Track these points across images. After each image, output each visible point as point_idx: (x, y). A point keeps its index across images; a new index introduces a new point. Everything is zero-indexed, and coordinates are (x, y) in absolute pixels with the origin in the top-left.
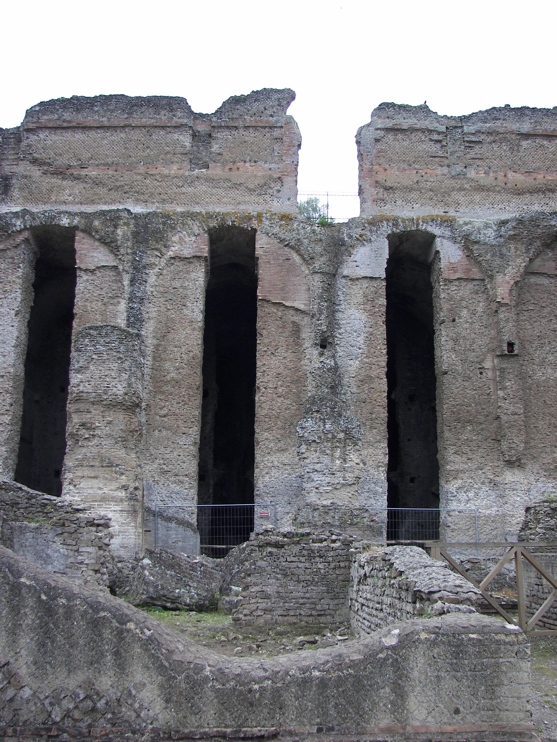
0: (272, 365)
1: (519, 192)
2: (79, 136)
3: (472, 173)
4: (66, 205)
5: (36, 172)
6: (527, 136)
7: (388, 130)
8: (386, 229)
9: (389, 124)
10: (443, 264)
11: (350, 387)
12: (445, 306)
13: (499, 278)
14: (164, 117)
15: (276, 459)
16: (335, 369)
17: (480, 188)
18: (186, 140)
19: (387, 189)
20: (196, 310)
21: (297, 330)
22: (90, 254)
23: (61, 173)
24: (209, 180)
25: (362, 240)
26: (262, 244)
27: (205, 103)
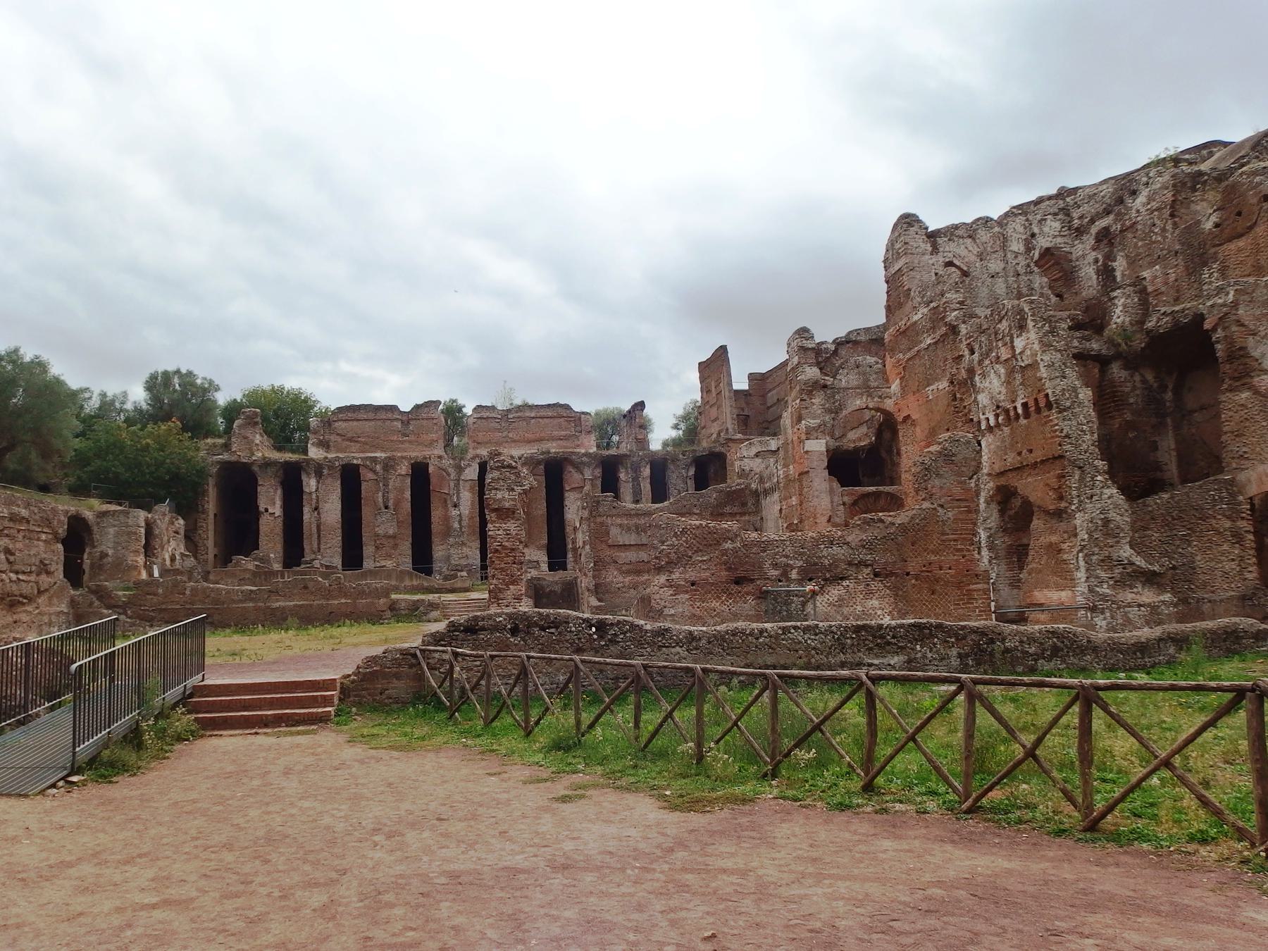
0: (436, 514)
1: (529, 442)
2: (355, 423)
4: (355, 456)
5: (339, 439)
8: (478, 460)
14: (390, 415)
15: (440, 548)
17: (514, 441)
18: (399, 424)
20: (408, 494)
21: (445, 501)
22: (366, 475)
23: (351, 440)
24: (410, 442)
25: (469, 465)
26: (431, 469)
27: (406, 407)
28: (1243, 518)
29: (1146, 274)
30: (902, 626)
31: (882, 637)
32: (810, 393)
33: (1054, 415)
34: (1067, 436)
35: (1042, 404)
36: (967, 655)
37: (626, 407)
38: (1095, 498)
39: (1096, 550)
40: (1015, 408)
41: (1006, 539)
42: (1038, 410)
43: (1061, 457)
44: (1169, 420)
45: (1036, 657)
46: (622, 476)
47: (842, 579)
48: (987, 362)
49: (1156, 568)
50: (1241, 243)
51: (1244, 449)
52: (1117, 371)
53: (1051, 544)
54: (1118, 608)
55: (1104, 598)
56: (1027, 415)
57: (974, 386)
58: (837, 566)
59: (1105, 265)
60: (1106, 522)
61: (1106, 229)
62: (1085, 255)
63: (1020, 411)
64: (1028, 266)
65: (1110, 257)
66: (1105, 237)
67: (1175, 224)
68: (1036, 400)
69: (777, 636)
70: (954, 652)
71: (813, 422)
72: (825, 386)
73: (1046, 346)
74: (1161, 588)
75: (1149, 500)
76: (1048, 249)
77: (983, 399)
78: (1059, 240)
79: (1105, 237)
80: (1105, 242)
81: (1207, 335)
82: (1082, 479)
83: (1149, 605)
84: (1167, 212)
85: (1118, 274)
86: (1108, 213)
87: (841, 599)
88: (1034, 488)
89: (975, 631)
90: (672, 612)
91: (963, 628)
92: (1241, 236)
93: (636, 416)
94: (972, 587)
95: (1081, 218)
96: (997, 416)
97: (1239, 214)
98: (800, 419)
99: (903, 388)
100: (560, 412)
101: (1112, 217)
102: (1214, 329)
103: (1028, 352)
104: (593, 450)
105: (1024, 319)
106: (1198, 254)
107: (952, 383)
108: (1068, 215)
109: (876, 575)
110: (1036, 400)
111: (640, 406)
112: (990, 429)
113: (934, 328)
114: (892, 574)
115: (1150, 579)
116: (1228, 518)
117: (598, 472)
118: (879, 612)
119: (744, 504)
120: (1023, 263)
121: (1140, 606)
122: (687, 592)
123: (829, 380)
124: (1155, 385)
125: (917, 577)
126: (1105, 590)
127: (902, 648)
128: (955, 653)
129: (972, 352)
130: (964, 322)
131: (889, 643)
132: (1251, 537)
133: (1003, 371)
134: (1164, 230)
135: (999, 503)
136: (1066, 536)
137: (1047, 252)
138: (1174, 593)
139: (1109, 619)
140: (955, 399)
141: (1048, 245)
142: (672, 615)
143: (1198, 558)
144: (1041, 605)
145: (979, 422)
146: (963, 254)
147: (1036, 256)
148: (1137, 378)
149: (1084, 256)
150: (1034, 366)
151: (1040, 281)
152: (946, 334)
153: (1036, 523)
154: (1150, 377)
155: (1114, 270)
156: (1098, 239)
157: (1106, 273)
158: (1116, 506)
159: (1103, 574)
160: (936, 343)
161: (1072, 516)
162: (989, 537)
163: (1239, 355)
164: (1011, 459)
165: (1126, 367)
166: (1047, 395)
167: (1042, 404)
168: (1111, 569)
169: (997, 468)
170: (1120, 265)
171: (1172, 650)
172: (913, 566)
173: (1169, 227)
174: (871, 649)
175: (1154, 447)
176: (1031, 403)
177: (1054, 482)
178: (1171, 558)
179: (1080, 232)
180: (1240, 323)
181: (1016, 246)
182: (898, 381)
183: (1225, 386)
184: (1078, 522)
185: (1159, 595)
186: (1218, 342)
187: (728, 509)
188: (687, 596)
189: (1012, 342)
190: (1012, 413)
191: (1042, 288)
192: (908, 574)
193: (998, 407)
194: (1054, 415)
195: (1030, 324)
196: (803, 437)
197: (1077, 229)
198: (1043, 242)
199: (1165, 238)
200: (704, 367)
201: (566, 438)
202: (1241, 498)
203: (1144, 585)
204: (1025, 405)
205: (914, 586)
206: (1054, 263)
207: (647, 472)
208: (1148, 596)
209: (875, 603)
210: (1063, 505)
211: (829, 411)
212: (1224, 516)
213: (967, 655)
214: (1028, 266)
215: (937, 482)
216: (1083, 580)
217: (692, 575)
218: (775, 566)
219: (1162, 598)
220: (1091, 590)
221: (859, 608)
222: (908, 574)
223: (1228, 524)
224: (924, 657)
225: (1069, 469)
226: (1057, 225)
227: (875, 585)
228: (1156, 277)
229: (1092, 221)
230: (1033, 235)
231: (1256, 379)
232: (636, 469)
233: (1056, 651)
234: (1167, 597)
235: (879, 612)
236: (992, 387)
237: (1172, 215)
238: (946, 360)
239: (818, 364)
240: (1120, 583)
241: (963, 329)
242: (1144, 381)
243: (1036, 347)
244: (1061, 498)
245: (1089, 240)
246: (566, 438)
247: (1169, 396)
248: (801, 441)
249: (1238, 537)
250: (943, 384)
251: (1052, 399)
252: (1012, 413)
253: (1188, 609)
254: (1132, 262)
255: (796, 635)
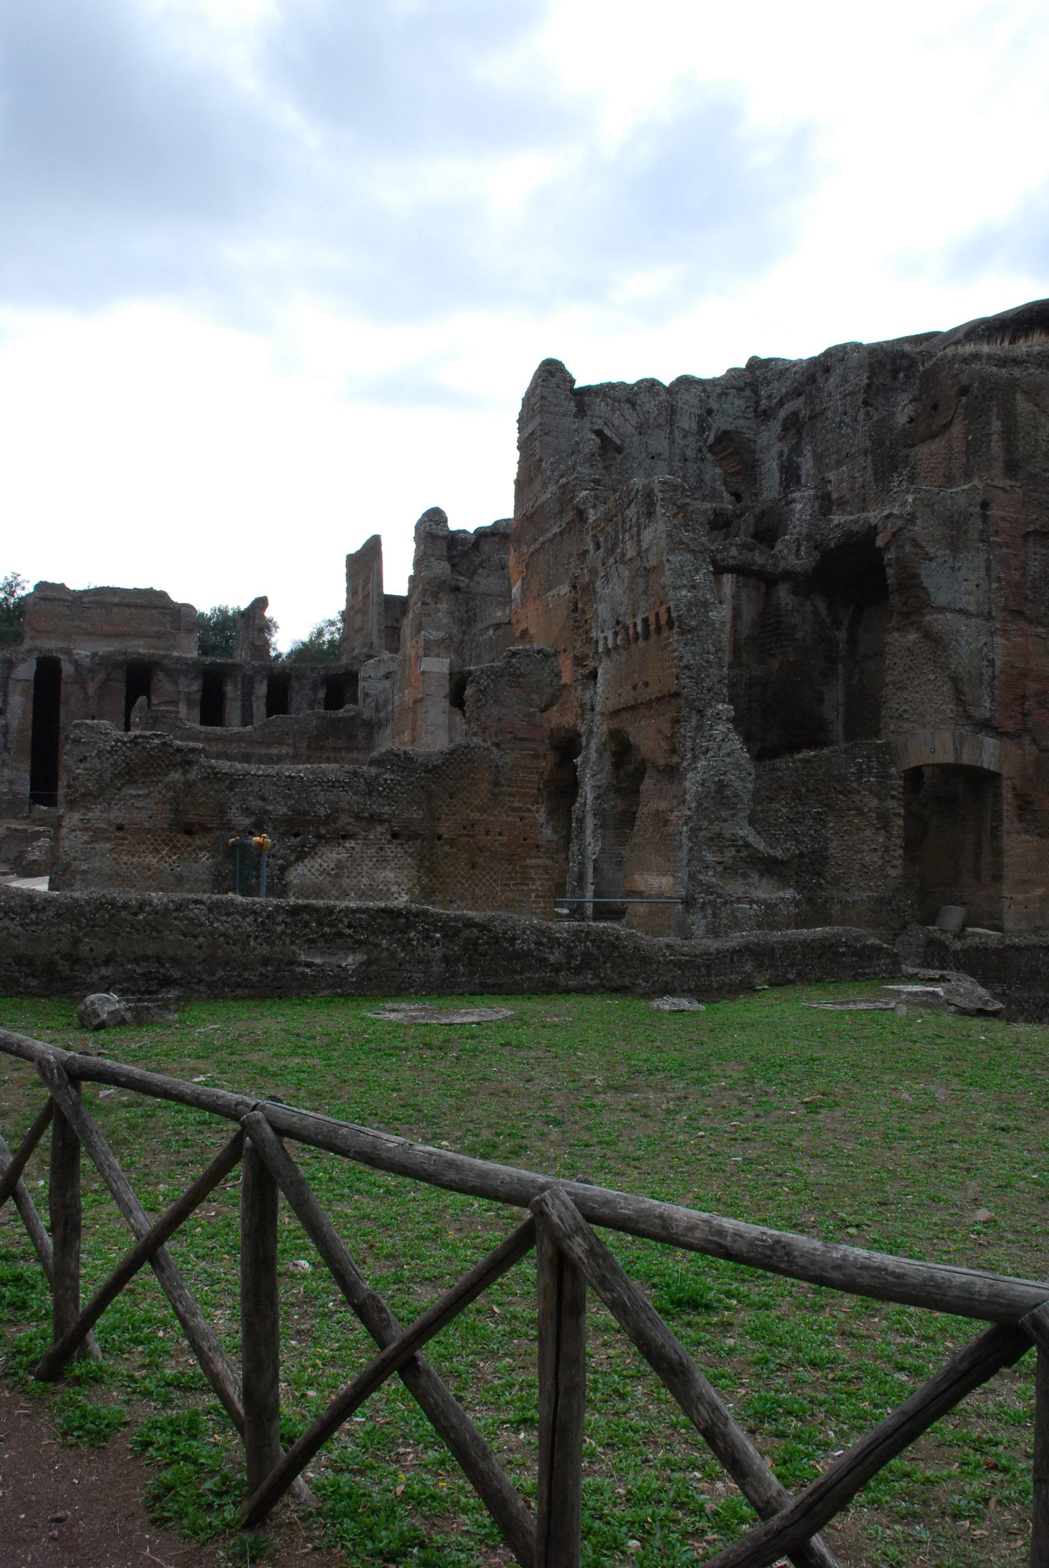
1: (108, 636)
3: (84, 625)
6: (116, 605)
7: (41, 599)
8: (36, 655)
9: (42, 595)
10: (64, 674)
11: (13, 735)
12: (63, 695)
13: (90, 683)
16: (6, 725)
17: (88, 633)
19: (39, 632)
25: (23, 660)
28: (893, 797)
29: (831, 476)
30: (367, 911)
31: (331, 925)
32: (435, 596)
33: (674, 636)
34: (687, 667)
35: (663, 621)
36: (457, 959)
37: (244, 605)
38: (711, 754)
39: (705, 824)
40: (635, 625)
41: (619, 802)
42: (659, 629)
43: (677, 695)
44: (840, 666)
45: (556, 969)
46: (229, 689)
47: (345, 837)
48: (611, 560)
49: (779, 853)
50: (934, 445)
51: (905, 707)
52: (784, 594)
53: (657, 812)
54: (724, 904)
55: (708, 889)
56: (647, 636)
57: (595, 592)
58: (337, 818)
59: (790, 460)
60: (721, 786)
61: (795, 414)
62: (770, 446)
63: (639, 629)
64: (700, 450)
65: (796, 450)
66: (793, 425)
67: (868, 414)
68: (657, 614)
69: (166, 912)
70: (439, 952)
71: (436, 635)
72: (457, 589)
73: (677, 545)
74: (784, 882)
75: (778, 762)
76: (726, 433)
77: (603, 610)
78: (742, 422)
79: (793, 425)
80: (793, 431)
81: (879, 553)
82: (699, 728)
83: (765, 902)
84: (860, 397)
85: (803, 472)
86: (799, 395)
87: (339, 866)
88: (647, 737)
89: (470, 924)
90: (84, 867)
91: (456, 919)
92: (933, 436)
93: (254, 619)
94: (528, 862)
95: (769, 397)
96: (616, 634)
97: (935, 407)
98: (420, 628)
99: (524, 590)
100: (152, 604)
101: (802, 398)
102: (887, 547)
103: (654, 550)
104: (195, 654)
105: (651, 504)
106: (889, 459)
107: (574, 587)
108: (756, 392)
109: (395, 835)
110: (657, 614)
111: (261, 603)
112: (608, 652)
113: (561, 512)
114: (414, 836)
115: (770, 867)
116: (876, 795)
117: (196, 686)
118: (394, 889)
119: (351, 737)
120: (694, 445)
121: (751, 902)
122: (109, 839)
123: (463, 581)
124: (828, 621)
125: (452, 843)
126: (709, 877)
127: (361, 943)
128: (439, 954)
129: (598, 547)
130: (594, 507)
131: (340, 935)
132: (901, 822)
133: (627, 573)
134: (855, 420)
135: (614, 754)
136: (675, 802)
137: (725, 437)
138: (799, 889)
139: (710, 918)
140: (575, 609)
141: (728, 427)
142: (84, 872)
143: (835, 844)
144: (641, 892)
145: (597, 642)
146: (617, 423)
147: (711, 440)
148: (808, 608)
149: (768, 448)
150: (657, 569)
151: (713, 472)
152: (573, 521)
153: (648, 784)
154: (822, 607)
155: (798, 468)
156: (785, 429)
157: (791, 475)
158: (737, 766)
159: (710, 857)
160: (562, 533)
161: (683, 777)
162: (596, 798)
163: (910, 582)
164: (628, 697)
165: (795, 592)
166: (669, 609)
167: (663, 621)
168: (721, 850)
169: (612, 705)
170: (807, 464)
171: (748, 967)
172: (445, 828)
173: (861, 415)
174: (312, 941)
175: (820, 701)
176: (652, 620)
177: (666, 727)
178: (799, 842)
179: (764, 415)
180: (915, 544)
181: (687, 422)
182: (519, 583)
183: (893, 623)
184: (687, 784)
185: (778, 890)
186: (890, 565)
187: (331, 742)
188: (108, 846)
189: (639, 534)
190: (631, 632)
191: (714, 481)
192: (440, 838)
193: (618, 623)
194: (674, 636)
195: (659, 510)
196: (421, 652)
197: (764, 412)
198: (720, 424)
199: (855, 431)
200: (353, 561)
201: (159, 636)
202: (893, 770)
203: (762, 875)
204: (645, 621)
205: (446, 855)
206: (732, 450)
207: (262, 689)
208: (765, 890)
209: (390, 875)
210: (675, 760)
211: (462, 622)
212: (871, 792)
213: (457, 959)
214: (700, 450)
215: (495, 711)
216: (684, 862)
217: (117, 815)
218: (247, 811)
219: (781, 894)
220: (692, 877)
221: (365, 880)
222: (440, 838)
223: (875, 803)
224: (393, 955)
225: (685, 711)
226: (739, 403)
227: (392, 850)
228: (842, 481)
229: (781, 403)
230: (710, 412)
231: (927, 618)
232: (249, 683)
233: (587, 962)
234: (789, 893)
235: (394, 889)
236: (613, 595)
237: (866, 403)
238: (571, 555)
239: (450, 558)
240: (728, 871)
241: (592, 516)
242: (816, 612)
243: (663, 543)
244: (674, 751)
245: (776, 426)
246: (159, 636)
247: (842, 635)
248: (418, 658)
249: (884, 820)
250: (564, 589)
251: (674, 615)
252: (631, 632)
253: (814, 912)
254: (818, 458)
255: (196, 910)
